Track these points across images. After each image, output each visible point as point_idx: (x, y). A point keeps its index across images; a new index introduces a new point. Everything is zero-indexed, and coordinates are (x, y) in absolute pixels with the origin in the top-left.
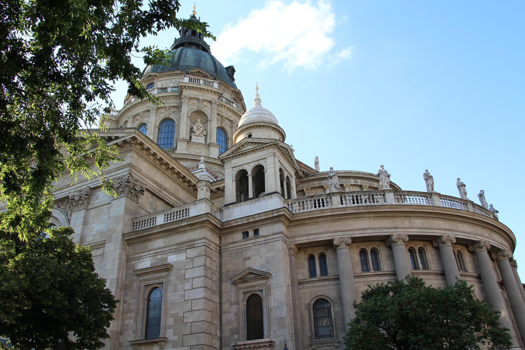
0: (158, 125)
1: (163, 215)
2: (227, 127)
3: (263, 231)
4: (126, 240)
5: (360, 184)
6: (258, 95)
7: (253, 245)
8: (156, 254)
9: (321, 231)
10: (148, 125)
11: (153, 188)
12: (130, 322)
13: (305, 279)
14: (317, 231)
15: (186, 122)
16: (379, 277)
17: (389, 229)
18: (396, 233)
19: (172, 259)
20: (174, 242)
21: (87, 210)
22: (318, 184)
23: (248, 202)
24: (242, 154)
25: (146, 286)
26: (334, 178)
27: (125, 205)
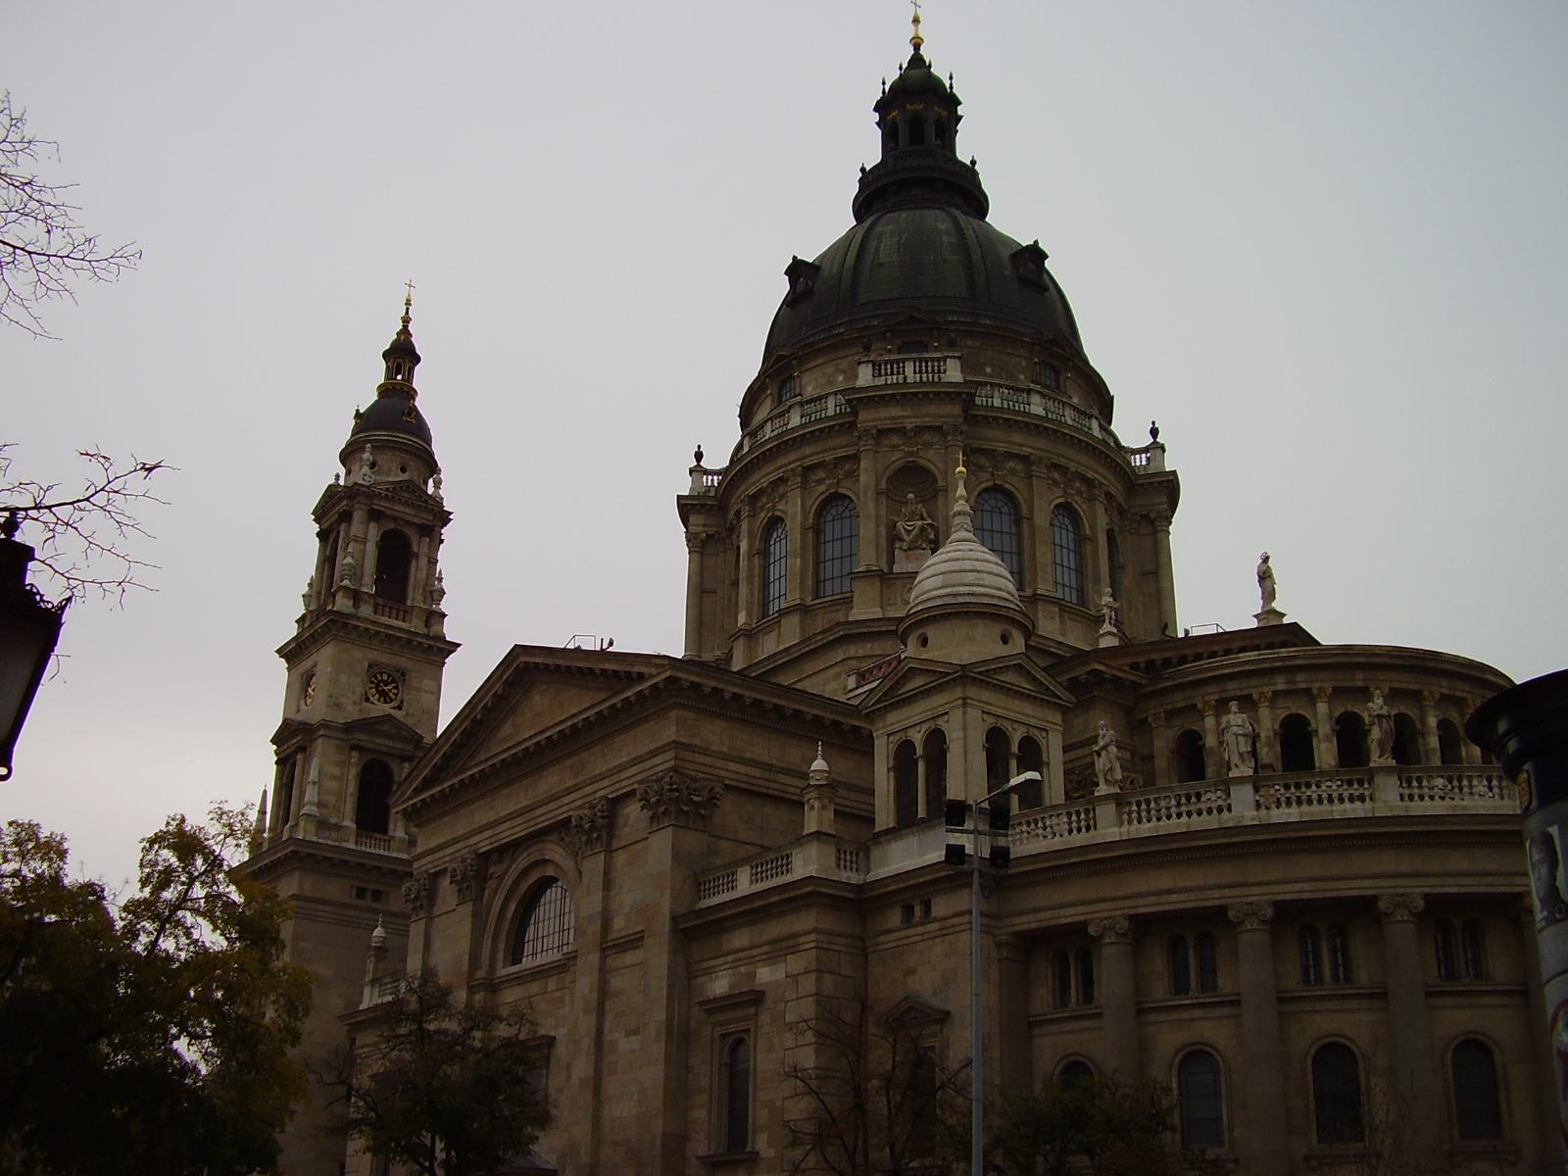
0: (811, 521)
1: (748, 867)
3: (941, 907)
4: (682, 930)
5: (1304, 686)
8: (736, 964)
11: (745, 779)
12: (700, 1114)
13: (1044, 1015)
15: (873, 513)
17: (1225, 888)
18: (1239, 900)
19: (765, 975)
21: (609, 851)
22: (1185, 699)
24: (903, 700)
25: (724, 1036)
26: (1104, 753)
27: (673, 848)
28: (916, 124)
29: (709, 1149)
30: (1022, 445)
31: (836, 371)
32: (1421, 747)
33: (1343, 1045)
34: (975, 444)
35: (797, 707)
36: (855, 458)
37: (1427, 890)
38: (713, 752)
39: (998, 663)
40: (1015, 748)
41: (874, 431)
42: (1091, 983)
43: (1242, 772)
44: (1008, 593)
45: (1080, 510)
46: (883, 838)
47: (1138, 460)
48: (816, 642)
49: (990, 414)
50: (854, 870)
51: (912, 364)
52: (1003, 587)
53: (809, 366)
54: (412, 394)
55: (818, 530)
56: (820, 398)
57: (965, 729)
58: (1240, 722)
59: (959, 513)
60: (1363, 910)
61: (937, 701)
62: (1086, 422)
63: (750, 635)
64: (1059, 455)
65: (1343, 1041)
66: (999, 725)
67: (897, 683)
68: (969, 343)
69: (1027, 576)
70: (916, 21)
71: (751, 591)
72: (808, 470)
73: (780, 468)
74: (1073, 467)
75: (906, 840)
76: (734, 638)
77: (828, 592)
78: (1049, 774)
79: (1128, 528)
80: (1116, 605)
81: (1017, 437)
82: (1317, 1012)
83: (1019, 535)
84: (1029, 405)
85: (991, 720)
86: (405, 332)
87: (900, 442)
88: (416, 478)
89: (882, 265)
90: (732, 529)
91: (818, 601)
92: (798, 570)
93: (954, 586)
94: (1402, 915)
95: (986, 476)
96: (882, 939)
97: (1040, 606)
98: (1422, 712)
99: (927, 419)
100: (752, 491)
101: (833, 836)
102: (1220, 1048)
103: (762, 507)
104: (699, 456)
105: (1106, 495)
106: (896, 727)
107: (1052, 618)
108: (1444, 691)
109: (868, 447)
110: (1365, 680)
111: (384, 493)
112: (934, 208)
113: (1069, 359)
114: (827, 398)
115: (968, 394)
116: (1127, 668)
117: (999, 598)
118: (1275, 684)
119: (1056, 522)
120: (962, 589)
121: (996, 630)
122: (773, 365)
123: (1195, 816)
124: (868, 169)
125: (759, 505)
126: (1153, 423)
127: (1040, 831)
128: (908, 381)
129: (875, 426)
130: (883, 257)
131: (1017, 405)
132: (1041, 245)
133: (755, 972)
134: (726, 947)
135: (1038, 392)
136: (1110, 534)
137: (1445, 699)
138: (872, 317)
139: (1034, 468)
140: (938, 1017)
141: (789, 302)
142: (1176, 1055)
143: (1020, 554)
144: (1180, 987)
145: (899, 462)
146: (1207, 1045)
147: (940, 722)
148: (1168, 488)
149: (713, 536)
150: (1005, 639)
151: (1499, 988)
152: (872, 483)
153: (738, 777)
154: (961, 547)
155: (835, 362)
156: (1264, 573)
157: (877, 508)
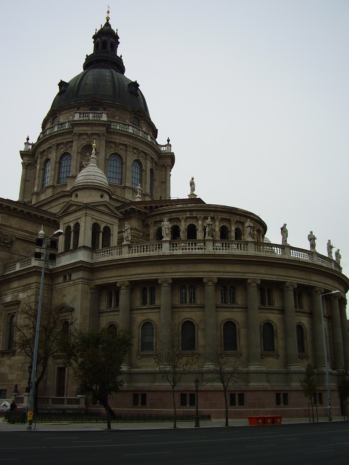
0: (58, 160)
1: (19, 263)
2: (122, 152)
5: (195, 216)
7: (67, 286)
9: (111, 275)
10: (51, 160)
13: (103, 310)
14: (108, 276)
15: (76, 158)
16: (152, 310)
18: (162, 277)
19: (21, 296)
20: (22, 284)
22: (160, 218)
23: (77, 250)
25: (9, 314)
26: (126, 232)
28: (104, 43)
29: (2, 349)
30: (125, 141)
31: (70, 115)
32: (229, 236)
33: (189, 321)
34: (110, 140)
35: (42, 215)
36: (72, 142)
37: (219, 277)
38: (14, 227)
39: (97, 203)
40: (102, 230)
41: (78, 134)
42: (118, 301)
43: (166, 239)
44: (104, 183)
45: (142, 162)
46: (60, 255)
47: (163, 149)
48: (55, 197)
49: (115, 131)
50: (51, 265)
52: (103, 181)
53: (62, 113)
55: (60, 163)
56: (64, 123)
57: (85, 223)
58: (167, 224)
59: (92, 158)
60: (199, 282)
61: (78, 214)
62: (146, 136)
63: (38, 194)
64: (136, 145)
65: (191, 320)
66: (97, 222)
67: (67, 208)
68: (111, 109)
69: (123, 180)
70: (108, 12)
71: (39, 181)
72: (58, 145)
73: (51, 143)
75: (66, 256)
76: (33, 194)
77: (62, 182)
78: (113, 238)
79: (158, 169)
80: (142, 189)
81: (123, 139)
82: (184, 311)
83: (122, 168)
84: (128, 129)
85: (94, 221)
87: (86, 138)
89: (87, 84)
90: (36, 162)
91: (58, 185)
92: (53, 175)
93: (87, 179)
94: (210, 283)
95: (113, 150)
96: (57, 286)
97: (126, 189)
98: (230, 225)
99: (95, 131)
100: (41, 150)
102: (154, 321)
103: (44, 155)
104: (28, 139)
105: (151, 158)
106: (66, 222)
107: (130, 193)
108: (238, 219)
109: (76, 139)
110: (214, 215)
112: (106, 69)
113: (144, 117)
114: (66, 123)
115: (108, 124)
117: (101, 184)
118: (187, 215)
119: (134, 165)
120: (89, 181)
121: (99, 193)
122: (52, 112)
123: (151, 251)
124: (88, 55)
125: (44, 155)
126: (168, 138)
127: (106, 255)
128: (90, 119)
129: (79, 132)
130: (88, 82)
131: (124, 129)
132: (137, 82)
133: (19, 295)
134: (11, 287)
135: (131, 126)
136: (151, 170)
137: (238, 222)
138: (82, 100)
139: (128, 148)
140: (70, 310)
141: (59, 94)
142: (141, 323)
143: (122, 174)
144: (144, 303)
145: (85, 144)
146: (151, 320)
147: (79, 221)
148: (171, 158)
149: (30, 164)
150: (102, 197)
151: (239, 306)
152: (76, 149)
153: (21, 236)
154: (91, 168)
155: (70, 113)
156: (192, 183)
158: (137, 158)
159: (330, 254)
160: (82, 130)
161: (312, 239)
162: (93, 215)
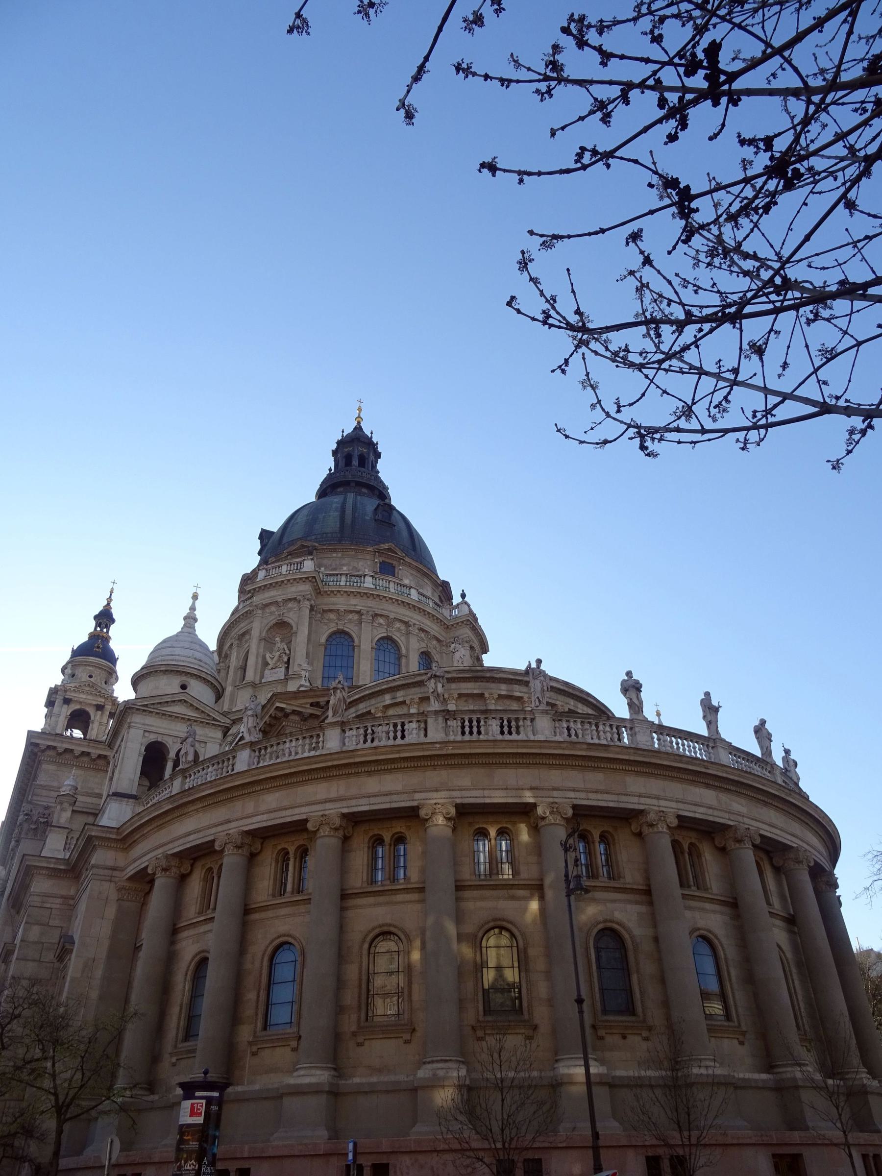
5: (401, 699)
6: (193, 608)
34: (325, 607)
51: (286, 566)
54: (107, 639)
64: (382, 609)
66: (159, 740)
68: (334, 555)
74: (392, 616)
81: (353, 601)
82: (277, 917)
85: (152, 738)
86: (108, 604)
88: (99, 680)
95: (333, 625)
101: (67, 828)
108: (503, 693)
111: (72, 689)
116: (308, 706)
139: (363, 617)
157: (258, 648)
158: (385, 635)
159: (713, 726)
160: (268, 598)
161: (710, 710)
162: (148, 725)
